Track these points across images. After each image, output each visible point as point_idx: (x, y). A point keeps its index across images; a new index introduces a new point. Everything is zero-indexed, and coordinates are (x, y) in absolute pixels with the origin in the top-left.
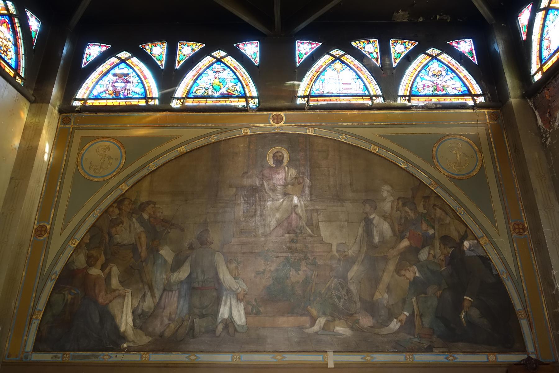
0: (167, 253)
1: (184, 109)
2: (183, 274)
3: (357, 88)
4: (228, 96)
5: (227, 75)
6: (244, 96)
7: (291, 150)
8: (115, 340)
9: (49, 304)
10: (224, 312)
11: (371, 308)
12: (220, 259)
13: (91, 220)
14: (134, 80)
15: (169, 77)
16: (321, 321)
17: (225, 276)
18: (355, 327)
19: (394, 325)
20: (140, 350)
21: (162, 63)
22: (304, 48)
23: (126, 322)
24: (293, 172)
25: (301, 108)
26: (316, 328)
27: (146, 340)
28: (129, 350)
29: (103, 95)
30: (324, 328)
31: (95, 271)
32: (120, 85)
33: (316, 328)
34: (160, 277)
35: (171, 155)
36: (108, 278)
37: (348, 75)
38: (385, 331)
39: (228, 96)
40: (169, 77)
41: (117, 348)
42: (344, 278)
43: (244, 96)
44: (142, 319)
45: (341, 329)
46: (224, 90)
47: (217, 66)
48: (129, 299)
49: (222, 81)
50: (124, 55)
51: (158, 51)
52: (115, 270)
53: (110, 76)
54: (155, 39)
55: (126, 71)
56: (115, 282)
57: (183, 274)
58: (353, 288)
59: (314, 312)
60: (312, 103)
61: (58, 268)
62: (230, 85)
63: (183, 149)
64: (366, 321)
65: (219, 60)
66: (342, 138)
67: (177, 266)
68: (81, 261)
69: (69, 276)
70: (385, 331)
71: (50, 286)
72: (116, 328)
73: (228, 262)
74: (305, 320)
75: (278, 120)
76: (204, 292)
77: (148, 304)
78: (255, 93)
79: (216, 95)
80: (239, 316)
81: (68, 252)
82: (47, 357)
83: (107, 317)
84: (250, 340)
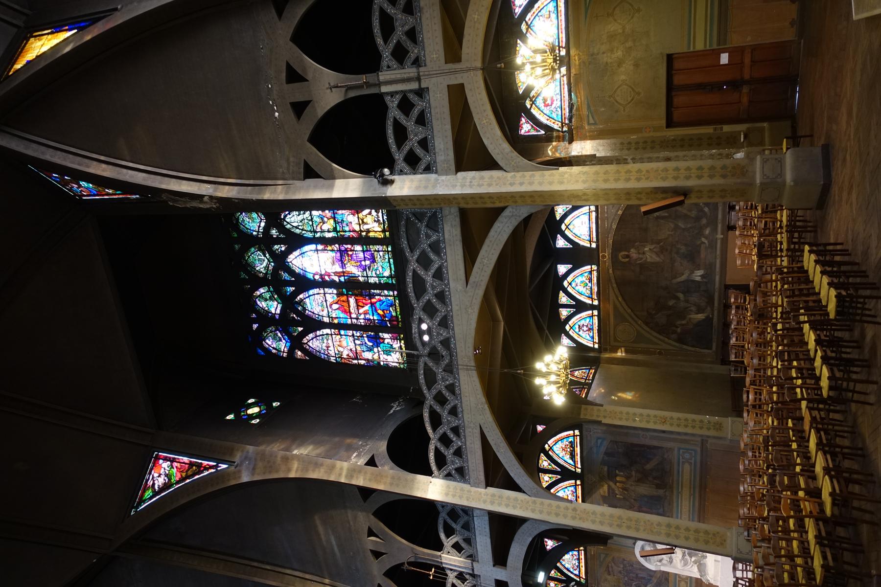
0: (671, 303)
1: (599, 300)
2: (681, 296)
3: (585, 218)
4: (590, 280)
5: (579, 280)
6: (591, 272)
7: (621, 251)
8: (709, 320)
9: (693, 346)
10: (698, 279)
11: (698, 219)
12: (675, 281)
13: (655, 334)
14: (581, 323)
15: (580, 307)
16: (703, 240)
17: (683, 278)
18: (706, 226)
19: (706, 209)
20: (713, 310)
21: (573, 310)
22: (561, 243)
23: (701, 316)
24: (632, 250)
25: (597, 246)
26: (706, 242)
27: (709, 308)
28: (713, 314)
29: (591, 334)
30: (706, 238)
31: (679, 330)
32: (585, 328)
33: (706, 242)
34: (682, 304)
35: (623, 303)
36: (683, 325)
37: (577, 222)
38: (709, 214)
39: (590, 280)
40: (580, 307)
41: (712, 318)
42: (684, 229)
43: (591, 272)
44: (700, 310)
45: (707, 232)
46: (587, 281)
47: (573, 284)
48: (692, 316)
49: (582, 282)
50: (567, 328)
51: (564, 313)
52: (679, 323)
53: (581, 333)
54: (558, 314)
55: (577, 326)
56: (684, 322)
57: (681, 296)
58: (689, 226)
59: (699, 243)
60: (595, 240)
61: (677, 344)
62: (584, 279)
63: (620, 299)
64: (704, 221)
65: (570, 284)
66: (614, 227)
67: (678, 298)
68: (674, 336)
69: (680, 340)
70: (709, 214)
71: (685, 347)
72: (704, 320)
73: (676, 278)
74: (703, 246)
75: (604, 256)
76: (689, 287)
77: (693, 308)
78: (589, 267)
79: (590, 285)
80: (700, 272)
81: (670, 341)
82: (714, 345)
83: (699, 323)
84: (710, 268)
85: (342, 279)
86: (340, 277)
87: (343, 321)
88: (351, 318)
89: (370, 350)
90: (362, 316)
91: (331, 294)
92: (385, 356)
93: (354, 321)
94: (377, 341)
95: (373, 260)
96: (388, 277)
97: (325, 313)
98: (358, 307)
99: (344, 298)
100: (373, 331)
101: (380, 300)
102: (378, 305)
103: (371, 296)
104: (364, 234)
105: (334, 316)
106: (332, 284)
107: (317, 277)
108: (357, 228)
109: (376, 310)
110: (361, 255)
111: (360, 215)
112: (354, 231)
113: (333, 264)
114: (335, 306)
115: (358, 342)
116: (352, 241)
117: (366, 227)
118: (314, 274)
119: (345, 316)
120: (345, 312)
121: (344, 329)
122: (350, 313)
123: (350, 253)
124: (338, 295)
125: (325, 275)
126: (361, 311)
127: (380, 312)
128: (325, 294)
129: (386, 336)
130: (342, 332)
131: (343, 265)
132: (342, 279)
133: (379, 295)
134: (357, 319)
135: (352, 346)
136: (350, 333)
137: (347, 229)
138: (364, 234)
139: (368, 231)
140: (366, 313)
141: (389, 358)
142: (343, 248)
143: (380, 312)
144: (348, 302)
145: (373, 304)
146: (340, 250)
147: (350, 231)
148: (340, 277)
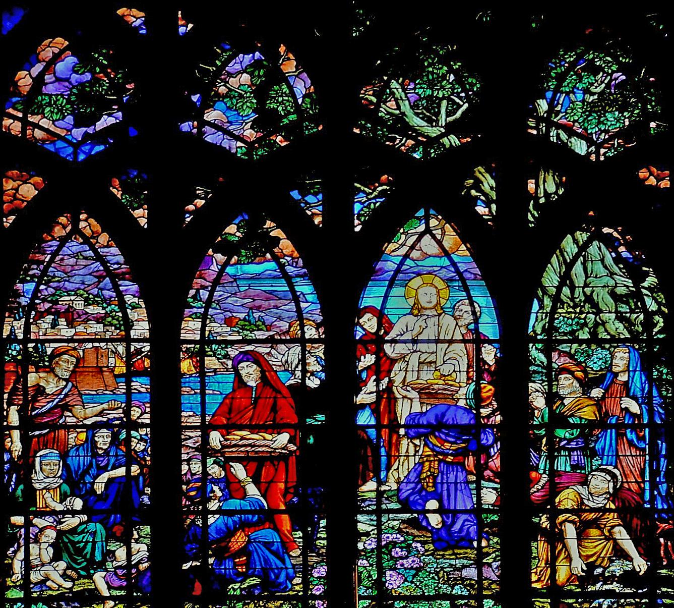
85: (365, 418)
86: (375, 408)
87: (189, 397)
88: (205, 429)
89: (75, 482)
90: (215, 471)
91: (301, 364)
92: (51, 535)
93: (193, 438)
94: (116, 511)
95: (445, 541)
96: (379, 584)
97: (217, 328)
98: (258, 463)
99: (289, 414)
100: (154, 499)
101: (287, 545)
102: (267, 534)
103: (302, 518)
104: (544, 522)
105: (211, 362)
106: (342, 378)
107: (369, 323)
108: (567, 499)
109: (244, 525)
110: (463, 502)
111: (612, 519)
112: (554, 489)
113: (426, 393)
114: (250, 373)
115: (103, 439)
116: (514, 479)
117: (570, 531)
118: (380, 315)
119: (212, 409)
120: (229, 405)
121: (154, 392)
122: (226, 429)
123: (470, 461)
124: (300, 389)
125: (379, 353)
126: (239, 471)
127: (239, 540)
128: (302, 341)
129: (141, 550)
130: (141, 384)
131: (418, 428)
132: (365, 418)
133: (309, 545)
134: (205, 450)
135: (89, 413)
136: (141, 414)
137: (562, 464)
138: (544, 522)
139: (555, 537)
140: (232, 487)
141: (42, 551)
142: (488, 438)
143: (239, 540)
144: (277, 429)
145: (267, 517)
146: (478, 427)
147: (553, 473)
148: (375, 408)
